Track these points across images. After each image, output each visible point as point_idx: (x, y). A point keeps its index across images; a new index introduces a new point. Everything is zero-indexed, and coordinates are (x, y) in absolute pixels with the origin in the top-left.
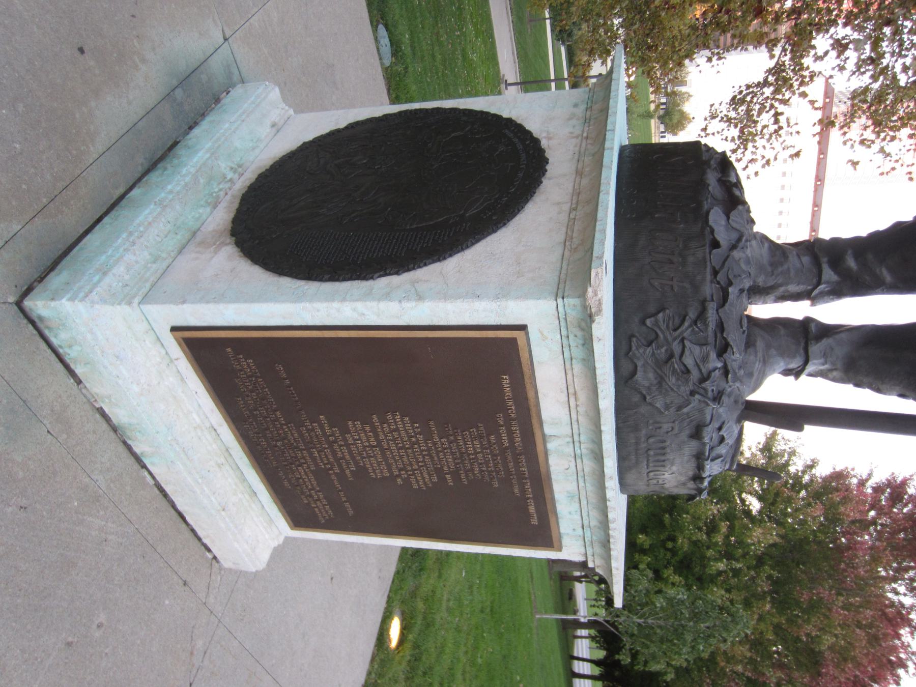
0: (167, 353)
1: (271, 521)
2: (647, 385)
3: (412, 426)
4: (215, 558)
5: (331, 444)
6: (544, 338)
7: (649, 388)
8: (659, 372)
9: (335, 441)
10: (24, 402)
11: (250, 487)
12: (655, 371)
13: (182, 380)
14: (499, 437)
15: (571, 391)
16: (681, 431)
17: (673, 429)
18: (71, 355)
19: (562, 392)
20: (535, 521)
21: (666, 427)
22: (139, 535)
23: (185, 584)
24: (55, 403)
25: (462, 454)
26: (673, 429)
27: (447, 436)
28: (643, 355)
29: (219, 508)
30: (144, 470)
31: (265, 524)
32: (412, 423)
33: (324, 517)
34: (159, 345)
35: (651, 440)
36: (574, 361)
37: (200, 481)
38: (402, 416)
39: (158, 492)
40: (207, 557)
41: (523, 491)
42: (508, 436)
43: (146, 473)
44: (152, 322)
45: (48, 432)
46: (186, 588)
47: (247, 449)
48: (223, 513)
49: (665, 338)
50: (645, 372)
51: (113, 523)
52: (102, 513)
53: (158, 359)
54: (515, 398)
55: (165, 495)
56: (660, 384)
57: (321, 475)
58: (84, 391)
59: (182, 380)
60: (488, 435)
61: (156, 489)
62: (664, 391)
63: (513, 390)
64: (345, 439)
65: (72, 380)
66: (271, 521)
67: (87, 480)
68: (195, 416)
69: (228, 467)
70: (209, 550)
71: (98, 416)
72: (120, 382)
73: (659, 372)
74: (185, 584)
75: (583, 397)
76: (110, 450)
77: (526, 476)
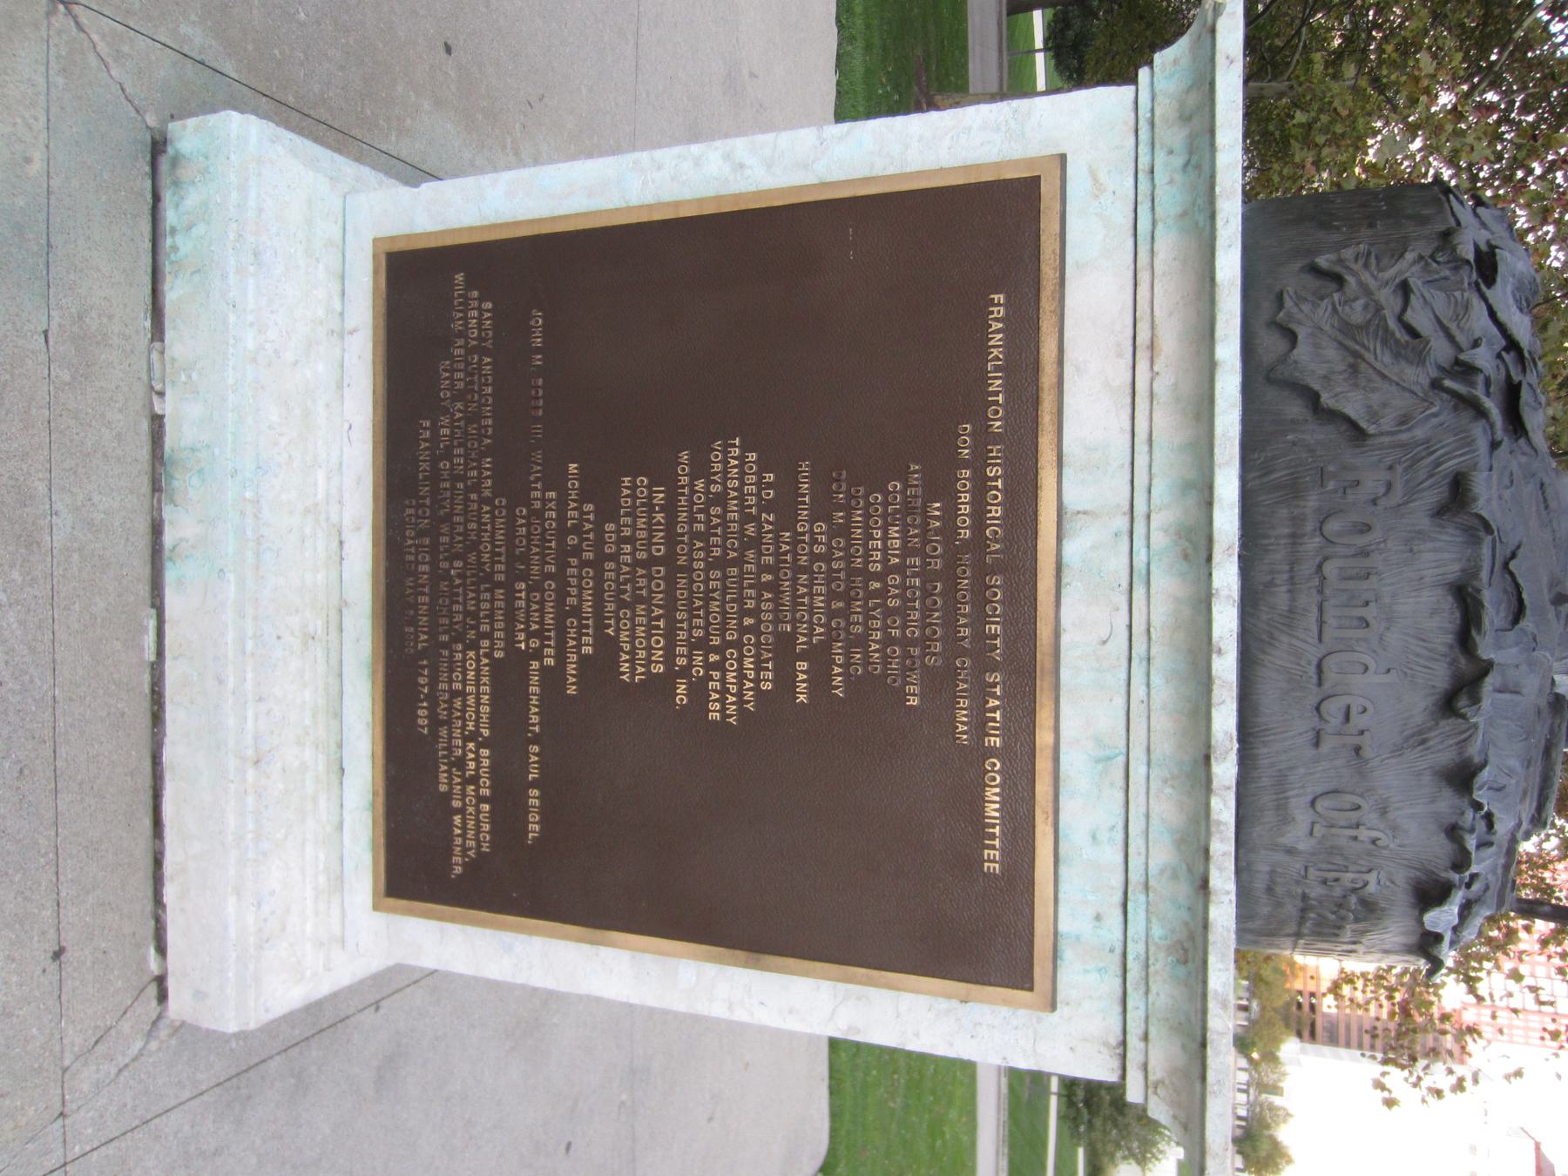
0: (342, 314)
1: (338, 882)
2: (1321, 372)
3: (759, 474)
4: (161, 980)
5: (564, 554)
6: (1098, 188)
7: (1326, 378)
8: (1350, 343)
9: (577, 551)
10: (49, 245)
11: (340, 746)
12: (1340, 343)
13: (340, 386)
14: (951, 511)
15: (1143, 336)
16: (1412, 492)
17: (1389, 486)
18: (181, 246)
19: (1120, 355)
20: (993, 859)
21: (1372, 482)
22: (48, 715)
23: (58, 955)
24: (94, 314)
25: (852, 573)
26: (1389, 486)
27: (828, 518)
28: (1315, 318)
29: (250, 752)
30: (153, 612)
31: (322, 879)
32: (763, 467)
33: (465, 849)
34: (337, 287)
35: (1333, 526)
36: (1160, 227)
37: (250, 645)
38: (745, 448)
39: (147, 689)
40: (144, 959)
41: (980, 725)
42: (972, 492)
43: (152, 624)
44: (349, 237)
45: (46, 333)
46: (53, 967)
47: (382, 588)
48: (251, 774)
49: (1361, 284)
50: (1317, 346)
51: (22, 623)
52: (16, 575)
53: (321, 313)
54: (1008, 369)
55: (157, 718)
56: (1354, 370)
57: (508, 677)
58: (155, 356)
59: (340, 386)
60: (927, 500)
61: (147, 678)
62: (1363, 383)
63: (1008, 345)
64: (599, 531)
65: (148, 324)
66: (338, 882)
67: (42, 488)
68: (321, 476)
69: (320, 654)
70: (162, 950)
71: (145, 425)
72: (232, 318)
73: (1350, 343)
74: (58, 955)
75: (1171, 341)
76: (117, 496)
77: (997, 655)
